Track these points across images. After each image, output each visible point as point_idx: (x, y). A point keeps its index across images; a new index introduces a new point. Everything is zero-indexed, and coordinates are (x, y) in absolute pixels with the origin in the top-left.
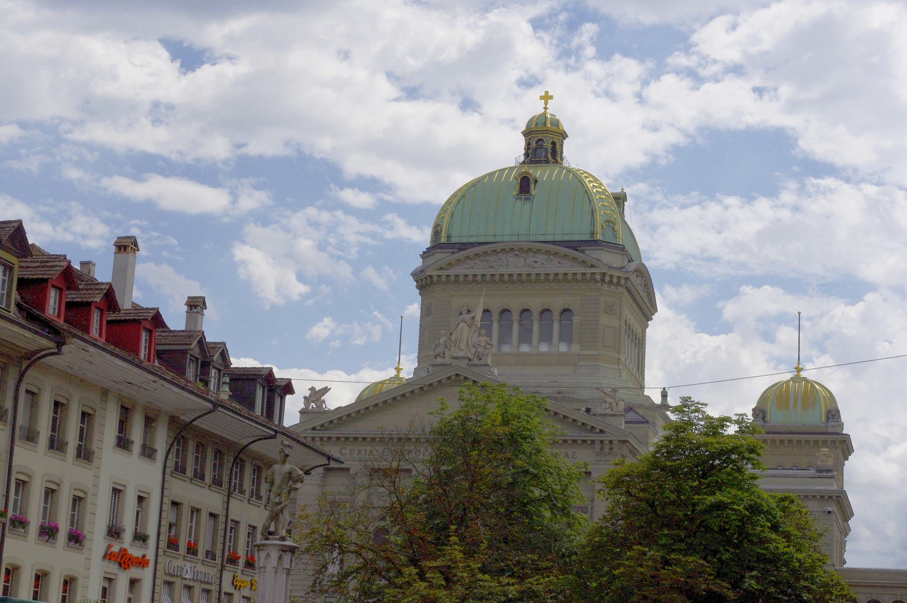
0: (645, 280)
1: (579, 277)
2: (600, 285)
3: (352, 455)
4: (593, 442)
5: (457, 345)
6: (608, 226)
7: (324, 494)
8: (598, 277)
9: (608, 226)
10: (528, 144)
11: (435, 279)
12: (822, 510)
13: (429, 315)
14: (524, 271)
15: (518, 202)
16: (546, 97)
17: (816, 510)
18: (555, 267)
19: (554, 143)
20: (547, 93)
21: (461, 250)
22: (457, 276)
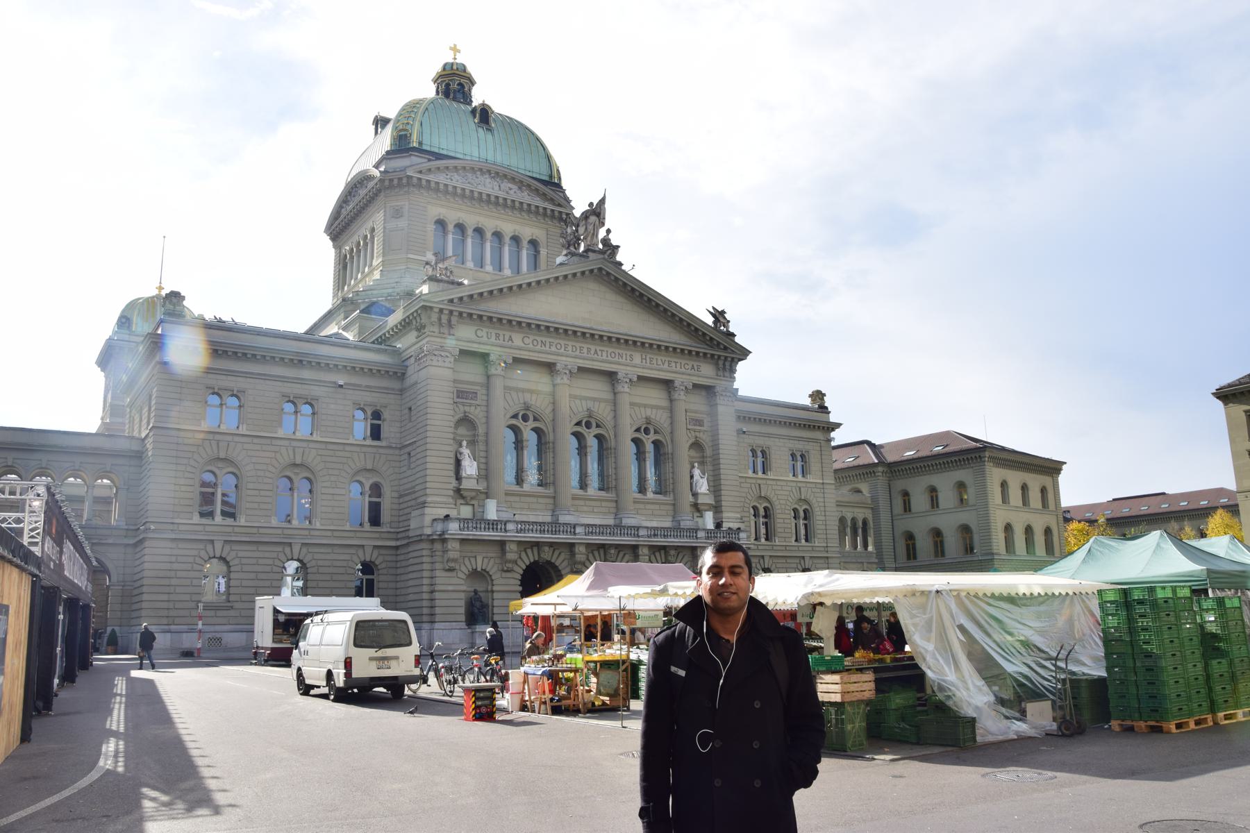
3: (488, 338)
4: (719, 356)
8: (564, 216)
13: (399, 217)
14: (502, 194)
15: (480, 130)
16: (455, 49)
20: (455, 45)
21: (437, 159)
22: (437, 183)
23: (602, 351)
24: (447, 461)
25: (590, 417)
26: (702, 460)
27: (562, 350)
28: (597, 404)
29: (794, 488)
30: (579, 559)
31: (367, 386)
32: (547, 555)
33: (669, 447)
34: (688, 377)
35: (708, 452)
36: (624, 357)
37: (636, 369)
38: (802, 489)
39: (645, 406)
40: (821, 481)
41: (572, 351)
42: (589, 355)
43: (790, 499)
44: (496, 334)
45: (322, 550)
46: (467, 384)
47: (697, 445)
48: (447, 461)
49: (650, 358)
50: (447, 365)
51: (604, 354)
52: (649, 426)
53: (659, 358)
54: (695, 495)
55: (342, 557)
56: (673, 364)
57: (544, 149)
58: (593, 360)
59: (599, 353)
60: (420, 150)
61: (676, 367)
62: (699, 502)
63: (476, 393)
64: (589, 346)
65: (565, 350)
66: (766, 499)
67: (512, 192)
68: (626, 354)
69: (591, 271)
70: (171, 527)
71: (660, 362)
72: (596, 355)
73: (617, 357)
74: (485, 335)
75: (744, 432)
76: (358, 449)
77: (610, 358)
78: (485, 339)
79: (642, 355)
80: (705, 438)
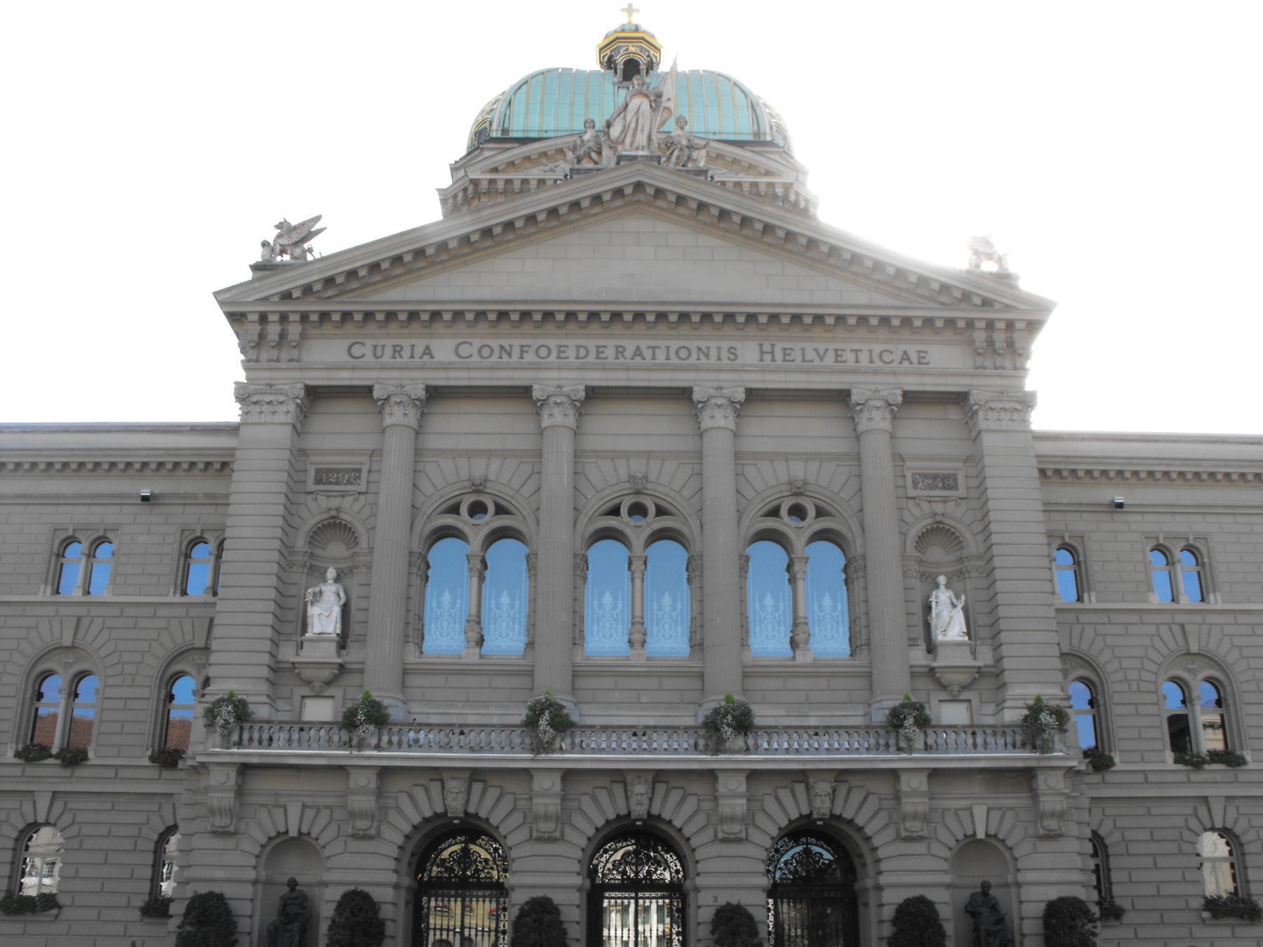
4: (970, 324)
5: (628, 140)
7: (300, 453)
8: (779, 191)
11: (484, 186)
20: (630, 6)
23: (654, 348)
24: (259, 606)
25: (638, 493)
26: (959, 567)
27: (553, 358)
30: (541, 810)
31: (207, 495)
32: (455, 801)
33: (859, 543)
34: (891, 379)
35: (973, 546)
36: (713, 354)
39: (787, 457)
41: (578, 357)
42: (622, 360)
44: (395, 346)
45: (94, 806)
47: (938, 532)
48: (259, 606)
49: (785, 349)
50: (283, 419)
52: (801, 501)
54: (931, 648)
55: (131, 819)
56: (850, 357)
57: (746, 96)
58: (628, 369)
59: (648, 354)
60: (506, 139)
61: (857, 361)
62: (934, 664)
63: (359, 471)
64: (619, 342)
65: (558, 357)
66: (1205, 657)
68: (719, 348)
69: (618, 192)
71: (811, 355)
72: (638, 359)
73: (694, 355)
75: (1120, 506)
76: (181, 612)
77: (674, 360)
78: (369, 358)
79: (761, 345)
80: (957, 514)
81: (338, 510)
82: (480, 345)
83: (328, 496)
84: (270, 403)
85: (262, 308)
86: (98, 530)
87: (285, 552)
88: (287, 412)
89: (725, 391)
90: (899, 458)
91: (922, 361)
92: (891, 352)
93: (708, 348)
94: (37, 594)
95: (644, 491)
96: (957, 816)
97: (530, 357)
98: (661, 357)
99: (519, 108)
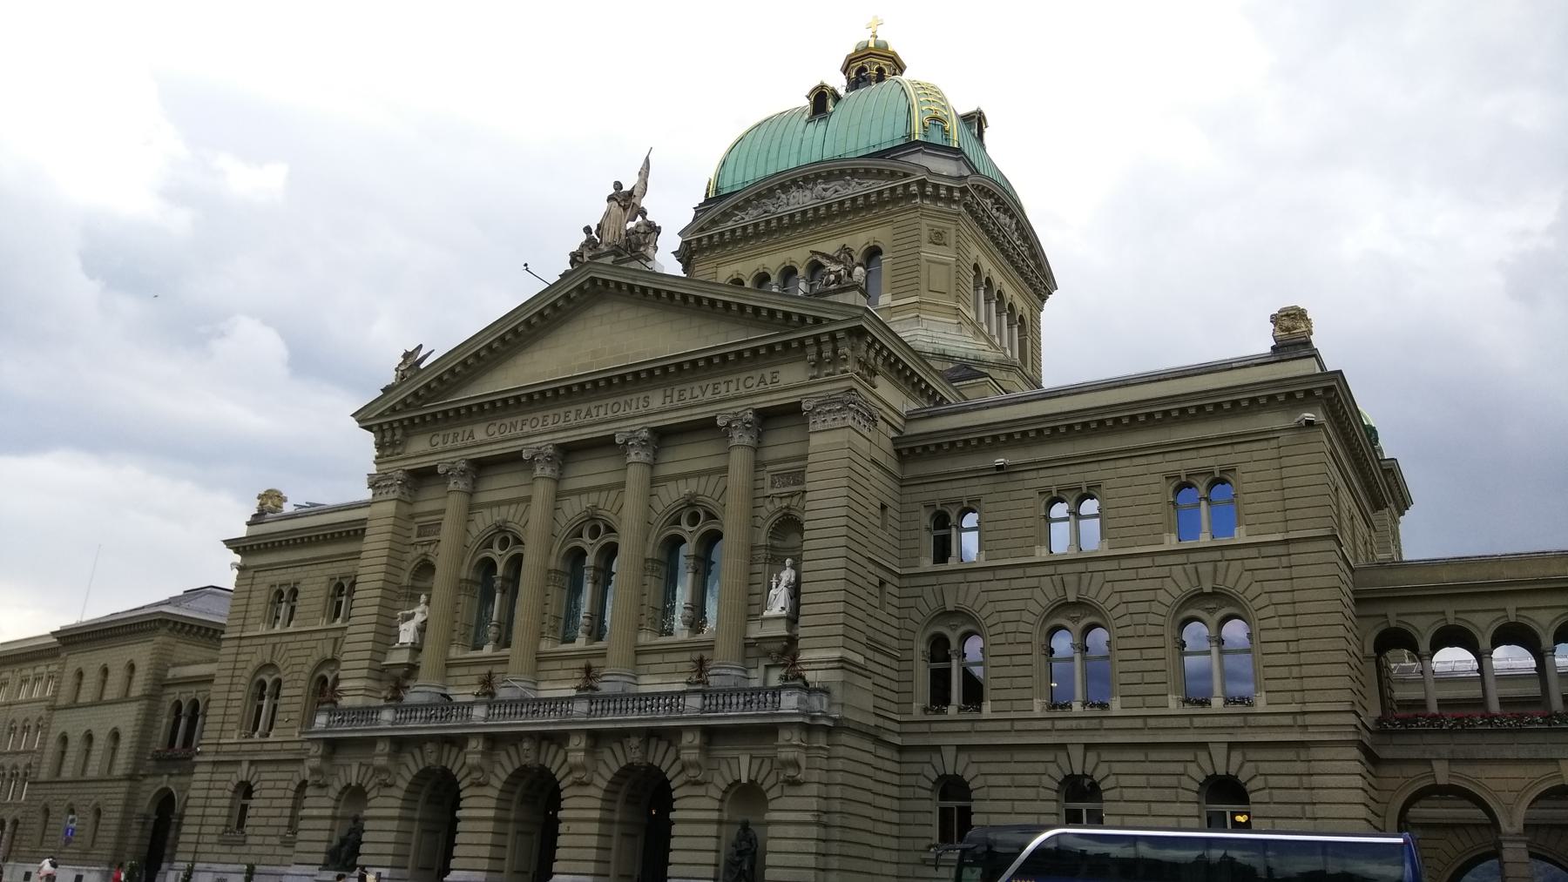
0: (1018, 222)
1: (886, 195)
2: (918, 200)
4: (801, 341)
6: (935, 125)
8: (914, 189)
9: (935, 125)
10: (848, 79)
12: (1293, 424)
15: (811, 126)
17: (1277, 426)
18: (855, 189)
19: (880, 70)
22: (722, 234)
28: (604, 494)
29: (1177, 571)
34: (749, 401)
36: (634, 406)
37: (651, 419)
38: (1201, 568)
39: (685, 476)
40: (1278, 537)
42: (579, 420)
43: (1162, 596)
46: (431, 515)
47: (789, 524)
50: (392, 496)
51: (602, 411)
53: (696, 385)
59: (594, 412)
67: (828, 194)
70: (213, 748)
71: (697, 392)
73: (622, 409)
74: (441, 442)
75: (999, 468)
81: (425, 554)
82: (498, 425)
83: (422, 545)
84: (385, 486)
85: (378, 422)
86: (350, 577)
87: (394, 587)
88: (394, 492)
89: (637, 433)
90: (758, 465)
91: (775, 380)
92: (753, 378)
93: (631, 400)
94: (317, 624)
95: (594, 516)
96: (728, 763)
97: (526, 429)
98: (602, 415)
99: (730, 166)
